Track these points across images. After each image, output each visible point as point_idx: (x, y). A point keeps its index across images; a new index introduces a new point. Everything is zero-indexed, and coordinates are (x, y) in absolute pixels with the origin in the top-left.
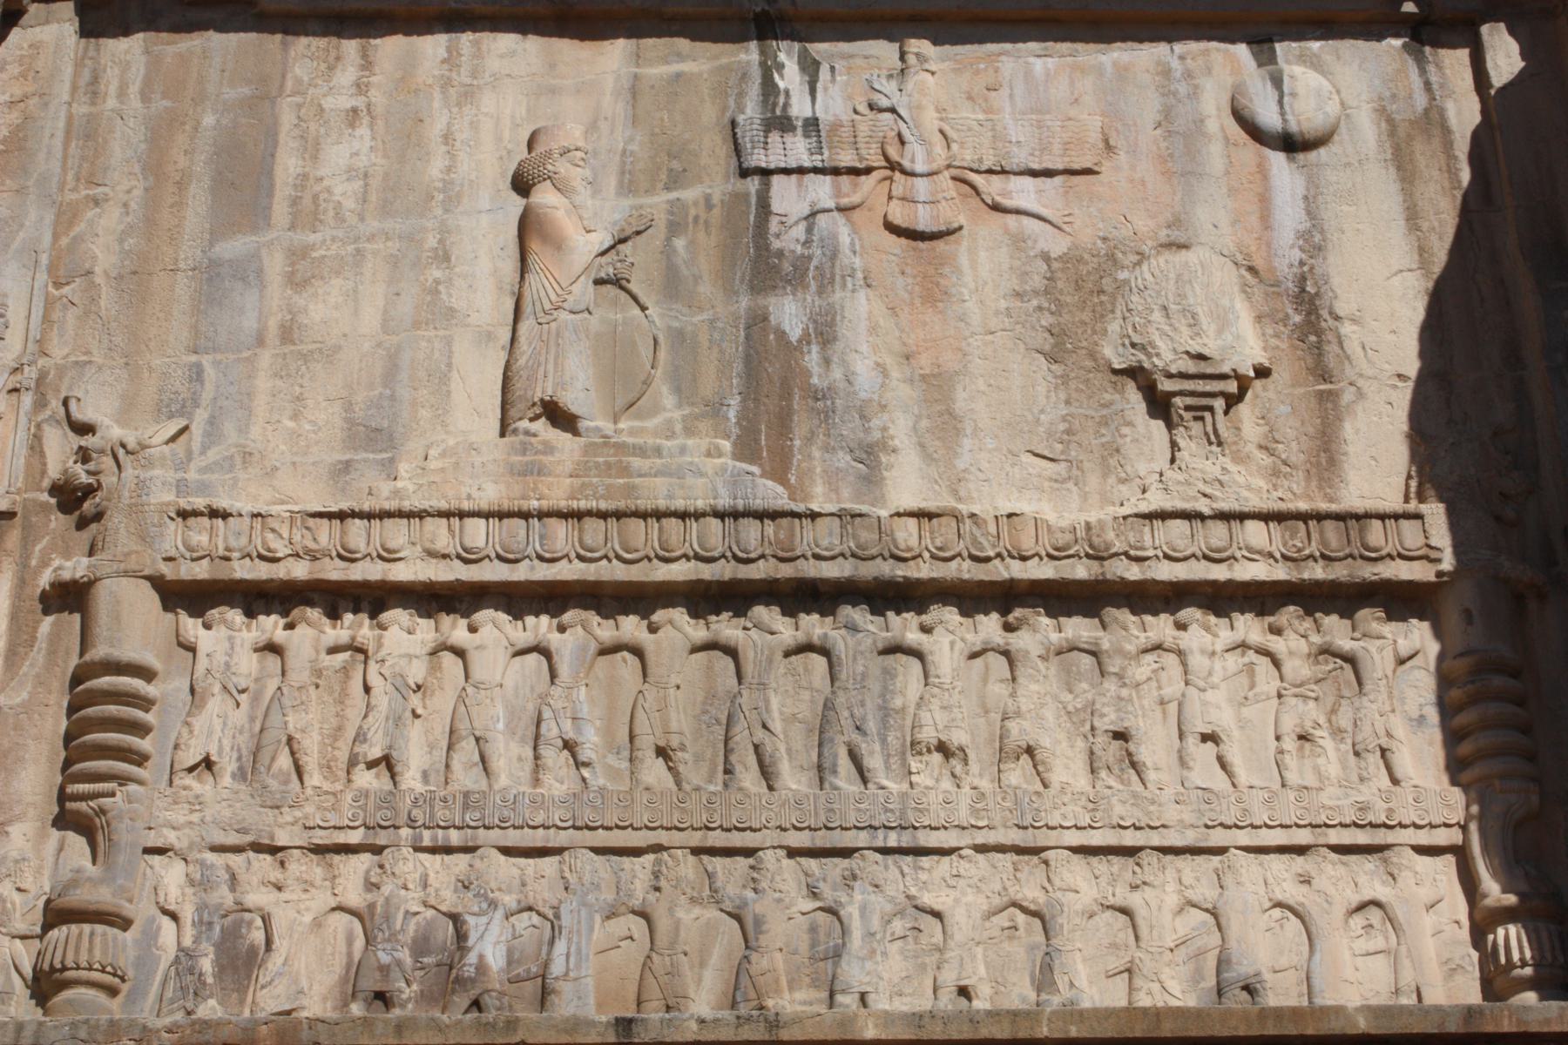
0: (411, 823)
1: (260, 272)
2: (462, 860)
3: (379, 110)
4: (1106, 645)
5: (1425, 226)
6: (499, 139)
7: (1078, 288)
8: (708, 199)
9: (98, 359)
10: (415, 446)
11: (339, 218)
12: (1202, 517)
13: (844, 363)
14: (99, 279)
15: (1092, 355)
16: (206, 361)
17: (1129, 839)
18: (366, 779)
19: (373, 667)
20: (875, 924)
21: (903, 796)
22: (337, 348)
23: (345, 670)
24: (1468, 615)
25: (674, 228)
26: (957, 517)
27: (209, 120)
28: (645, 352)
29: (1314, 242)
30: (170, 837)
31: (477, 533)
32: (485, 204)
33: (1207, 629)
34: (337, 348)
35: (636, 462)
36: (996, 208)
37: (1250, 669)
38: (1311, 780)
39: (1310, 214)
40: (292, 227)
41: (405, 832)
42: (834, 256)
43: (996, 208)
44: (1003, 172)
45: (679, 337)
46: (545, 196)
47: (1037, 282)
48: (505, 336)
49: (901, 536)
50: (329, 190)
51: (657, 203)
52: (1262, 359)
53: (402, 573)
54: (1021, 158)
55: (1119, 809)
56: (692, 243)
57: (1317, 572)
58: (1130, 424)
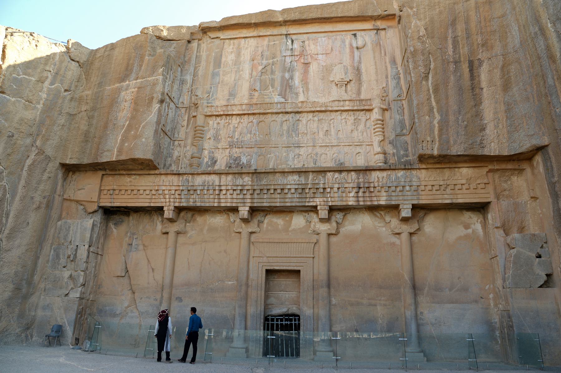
0: (235, 145)
1: (219, 74)
2: (241, 150)
3: (235, 51)
4: (326, 119)
5: (376, 59)
6: (250, 54)
7: (327, 70)
8: (277, 60)
9: (199, 87)
10: (238, 96)
11: (229, 66)
12: (340, 101)
13: (294, 82)
14: (199, 76)
15: (328, 79)
16: (212, 86)
17: (328, 145)
18: (229, 139)
19: (231, 125)
20: (293, 156)
21: (298, 140)
22: (228, 83)
23: (228, 125)
24: (376, 113)
25: (273, 64)
26: (307, 102)
27: (214, 54)
28: (268, 82)
29: (360, 62)
30: (206, 147)
31: (244, 107)
32: (248, 63)
33: (341, 116)
34: (228, 83)
35: (265, 97)
36: (316, 59)
37: (346, 122)
38: (353, 136)
39: (360, 58)
40: (223, 68)
41: (234, 146)
42: (294, 67)
43: (316, 59)
44: (317, 54)
45: (272, 79)
46: (255, 62)
47: (321, 69)
48: (249, 80)
49: (299, 105)
50: (228, 63)
51: (271, 61)
52: (351, 79)
53: (234, 113)
54: (319, 52)
55: (327, 141)
56: (275, 67)
57: (356, 108)
58: (332, 88)
